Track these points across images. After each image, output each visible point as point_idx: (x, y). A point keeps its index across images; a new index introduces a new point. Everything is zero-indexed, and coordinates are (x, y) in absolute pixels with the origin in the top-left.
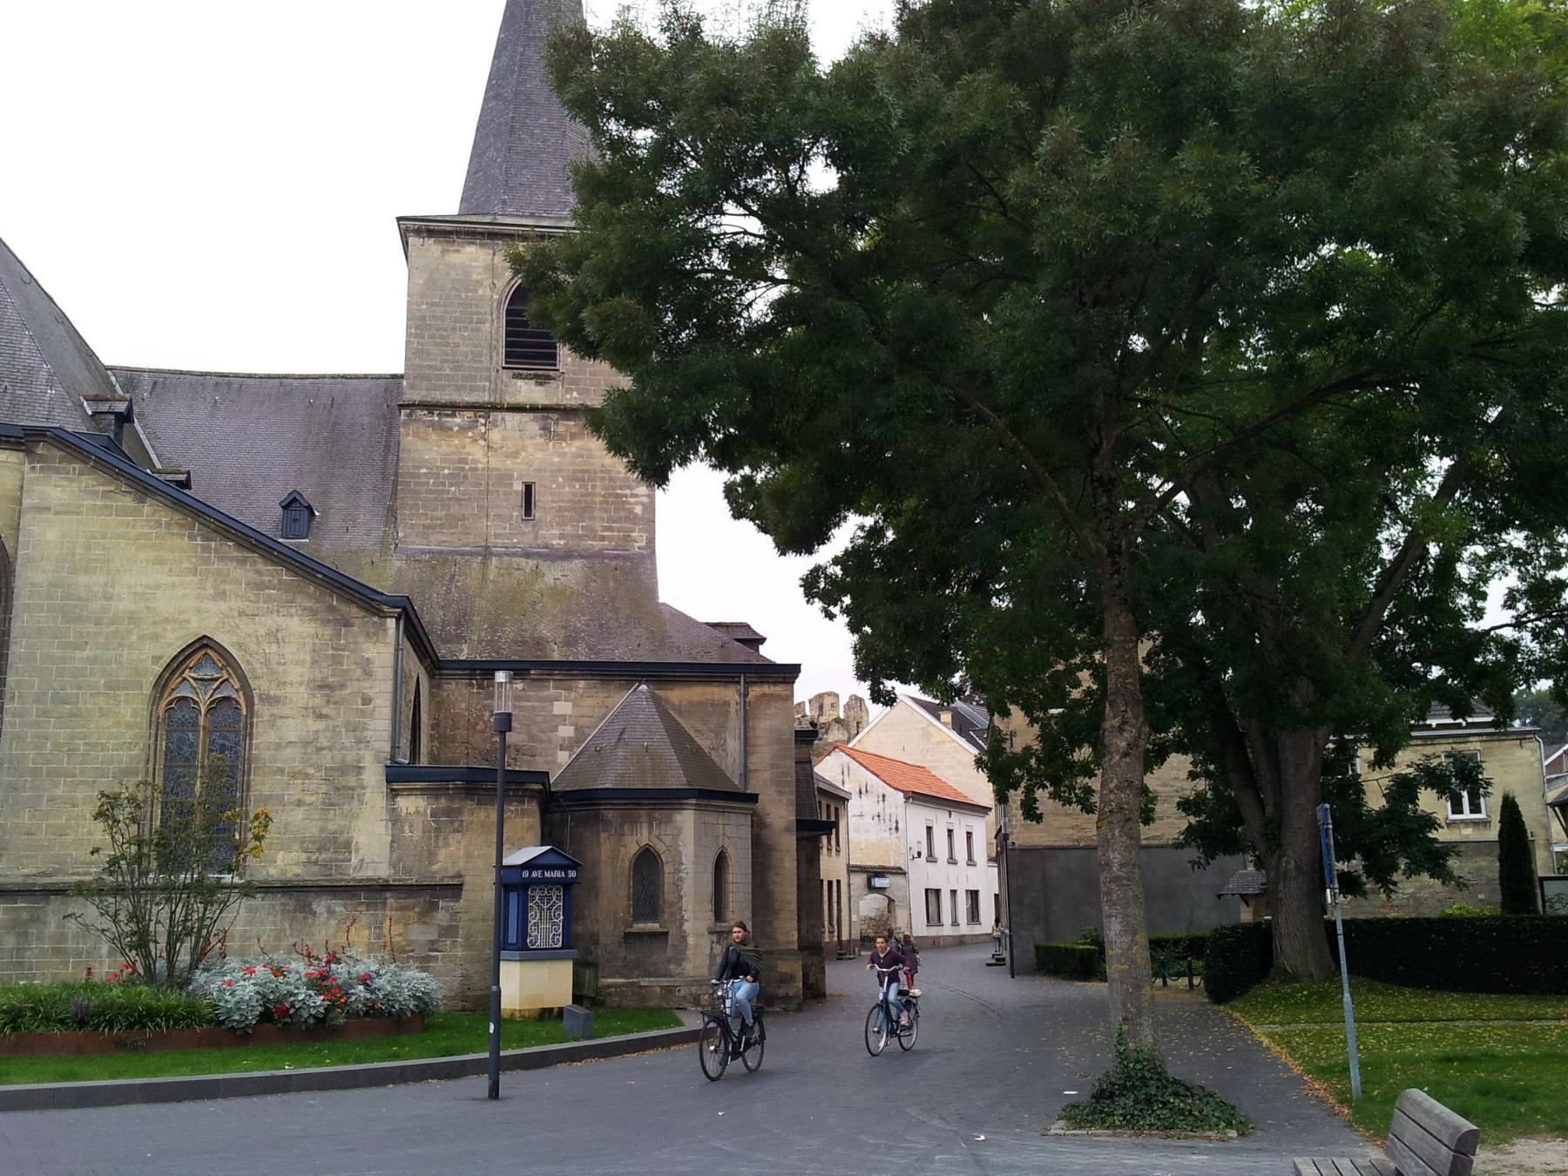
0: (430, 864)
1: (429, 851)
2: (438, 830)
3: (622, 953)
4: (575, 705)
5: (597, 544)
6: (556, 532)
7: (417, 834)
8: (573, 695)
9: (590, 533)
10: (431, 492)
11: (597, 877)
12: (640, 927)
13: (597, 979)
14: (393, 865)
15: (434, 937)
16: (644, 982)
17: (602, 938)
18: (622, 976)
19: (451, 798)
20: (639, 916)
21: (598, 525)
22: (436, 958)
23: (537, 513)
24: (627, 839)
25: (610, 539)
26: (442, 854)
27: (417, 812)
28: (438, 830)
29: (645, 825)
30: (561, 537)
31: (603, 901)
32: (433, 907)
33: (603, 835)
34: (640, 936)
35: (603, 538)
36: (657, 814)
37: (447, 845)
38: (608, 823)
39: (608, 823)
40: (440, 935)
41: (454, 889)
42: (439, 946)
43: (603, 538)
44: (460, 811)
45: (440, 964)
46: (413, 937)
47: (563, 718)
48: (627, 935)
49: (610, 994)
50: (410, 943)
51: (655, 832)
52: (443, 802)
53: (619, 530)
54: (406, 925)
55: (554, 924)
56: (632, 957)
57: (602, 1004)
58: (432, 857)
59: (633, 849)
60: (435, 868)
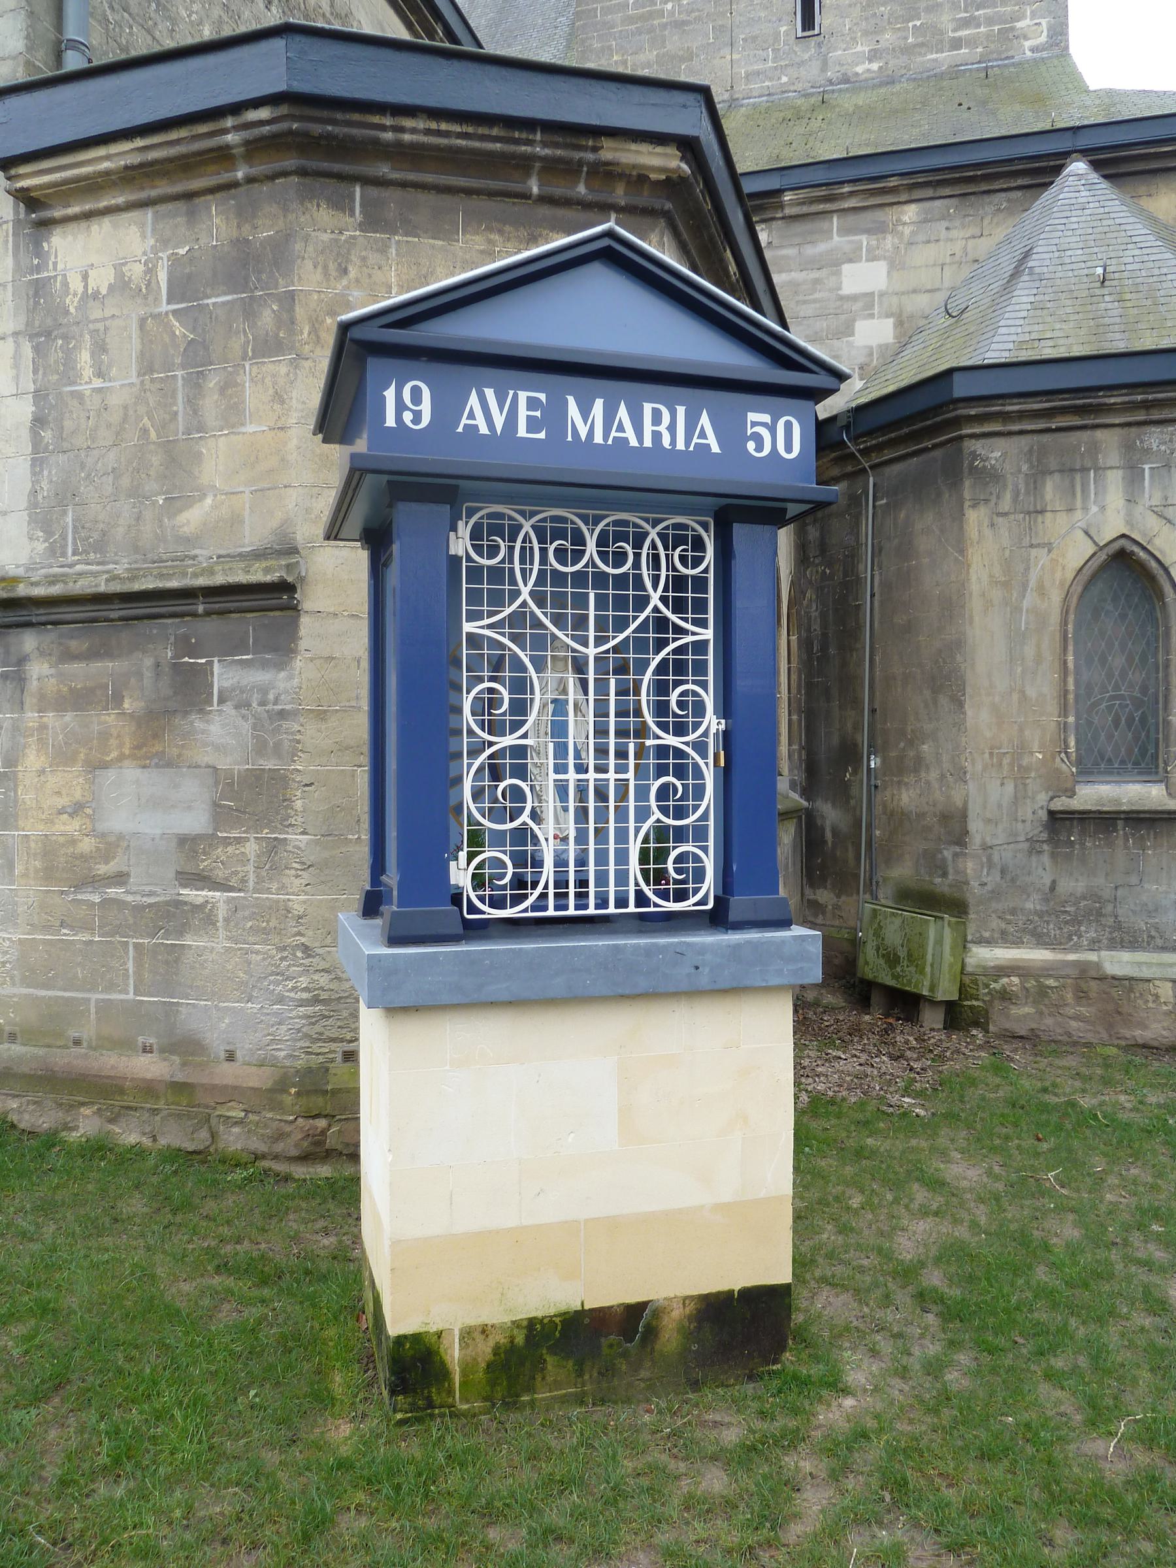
0: (176, 503)
1: (168, 447)
2: (198, 356)
3: (1043, 871)
4: (895, 265)
5: (943, 58)
6: (863, 48)
7: (125, 378)
8: (889, 241)
9: (933, 39)
10: (631, 20)
11: (958, 645)
12: (1096, 794)
13: (963, 945)
14: (43, 518)
15: (195, 821)
16: (1119, 962)
17: (975, 826)
18: (1041, 940)
19: (245, 214)
20: (1092, 764)
21: (945, 20)
22: (204, 916)
23: (823, 20)
24: (1055, 524)
25: (971, 42)
26: (217, 460)
27: (121, 285)
28: (198, 356)
29: (1115, 480)
30: (873, 56)
31: (979, 716)
32: (189, 690)
33: (975, 518)
34: (1103, 822)
35: (956, 44)
36: (1154, 438)
37: (234, 415)
38: (989, 477)
39: (989, 477)
40: (220, 814)
41: (264, 603)
42: (213, 862)
43: (956, 44)
44: (279, 256)
45: (220, 941)
46: (119, 821)
47: (867, 300)
48: (1057, 820)
49: (1005, 996)
50: (110, 846)
51: (1151, 494)
52: (217, 225)
53: (990, 21)
54: (95, 766)
55: (671, 762)
56: (1073, 884)
57: (979, 1020)
58: (177, 465)
59: (1077, 553)
60: (192, 518)
